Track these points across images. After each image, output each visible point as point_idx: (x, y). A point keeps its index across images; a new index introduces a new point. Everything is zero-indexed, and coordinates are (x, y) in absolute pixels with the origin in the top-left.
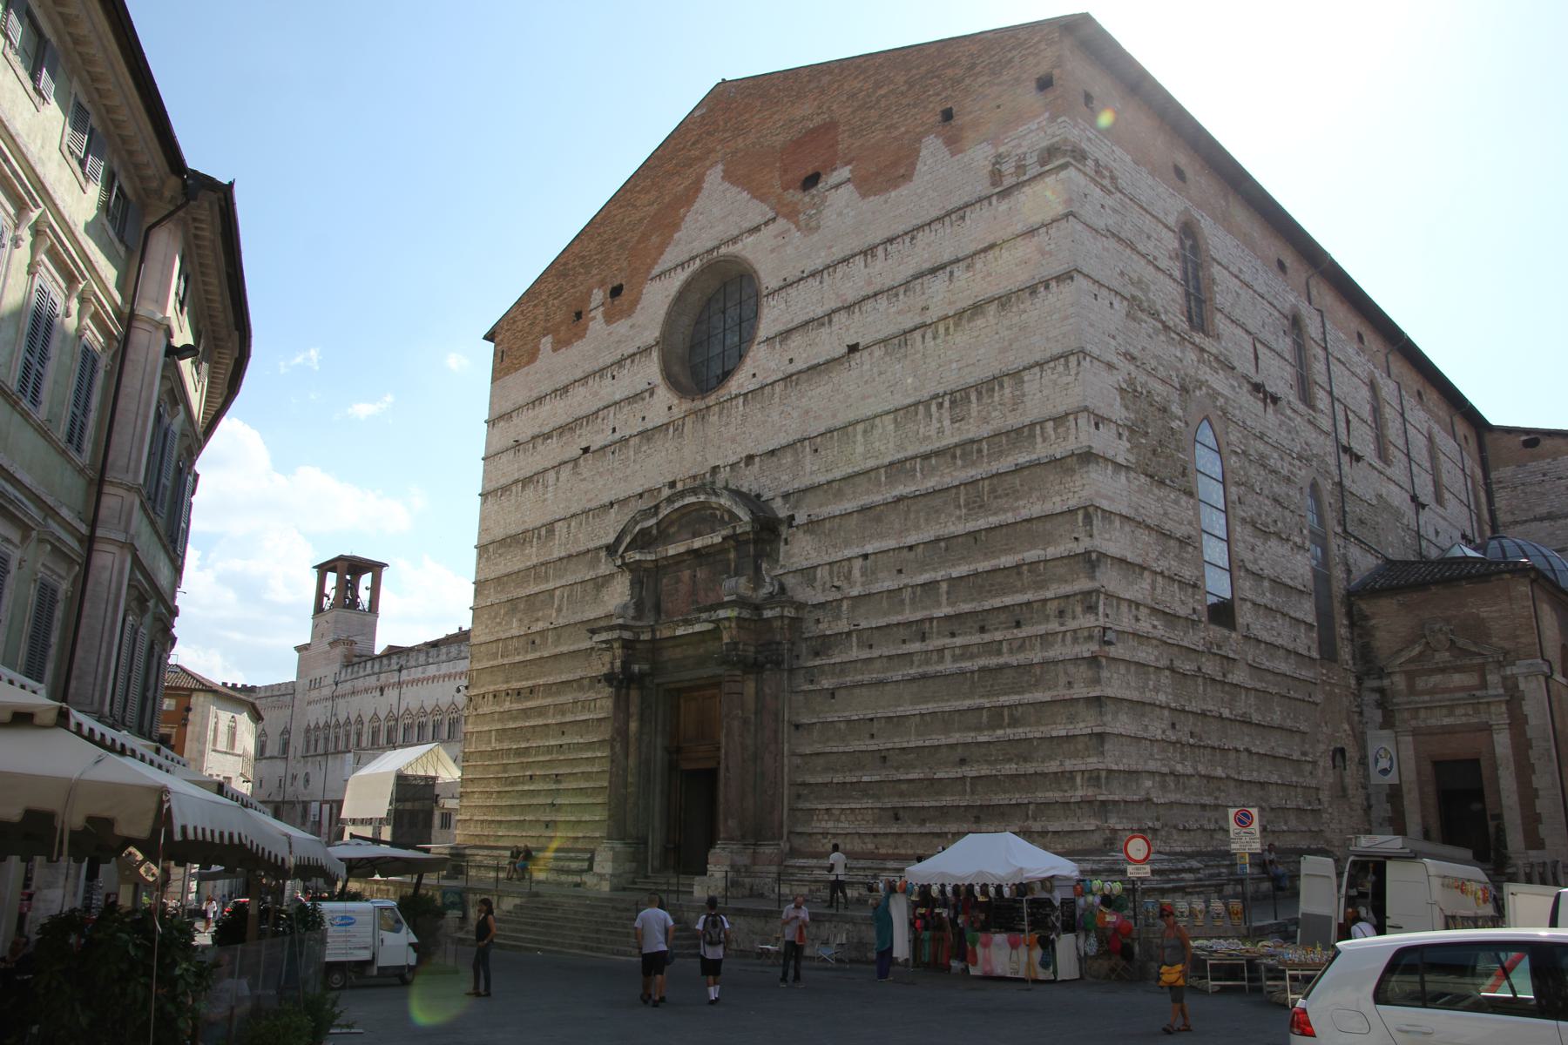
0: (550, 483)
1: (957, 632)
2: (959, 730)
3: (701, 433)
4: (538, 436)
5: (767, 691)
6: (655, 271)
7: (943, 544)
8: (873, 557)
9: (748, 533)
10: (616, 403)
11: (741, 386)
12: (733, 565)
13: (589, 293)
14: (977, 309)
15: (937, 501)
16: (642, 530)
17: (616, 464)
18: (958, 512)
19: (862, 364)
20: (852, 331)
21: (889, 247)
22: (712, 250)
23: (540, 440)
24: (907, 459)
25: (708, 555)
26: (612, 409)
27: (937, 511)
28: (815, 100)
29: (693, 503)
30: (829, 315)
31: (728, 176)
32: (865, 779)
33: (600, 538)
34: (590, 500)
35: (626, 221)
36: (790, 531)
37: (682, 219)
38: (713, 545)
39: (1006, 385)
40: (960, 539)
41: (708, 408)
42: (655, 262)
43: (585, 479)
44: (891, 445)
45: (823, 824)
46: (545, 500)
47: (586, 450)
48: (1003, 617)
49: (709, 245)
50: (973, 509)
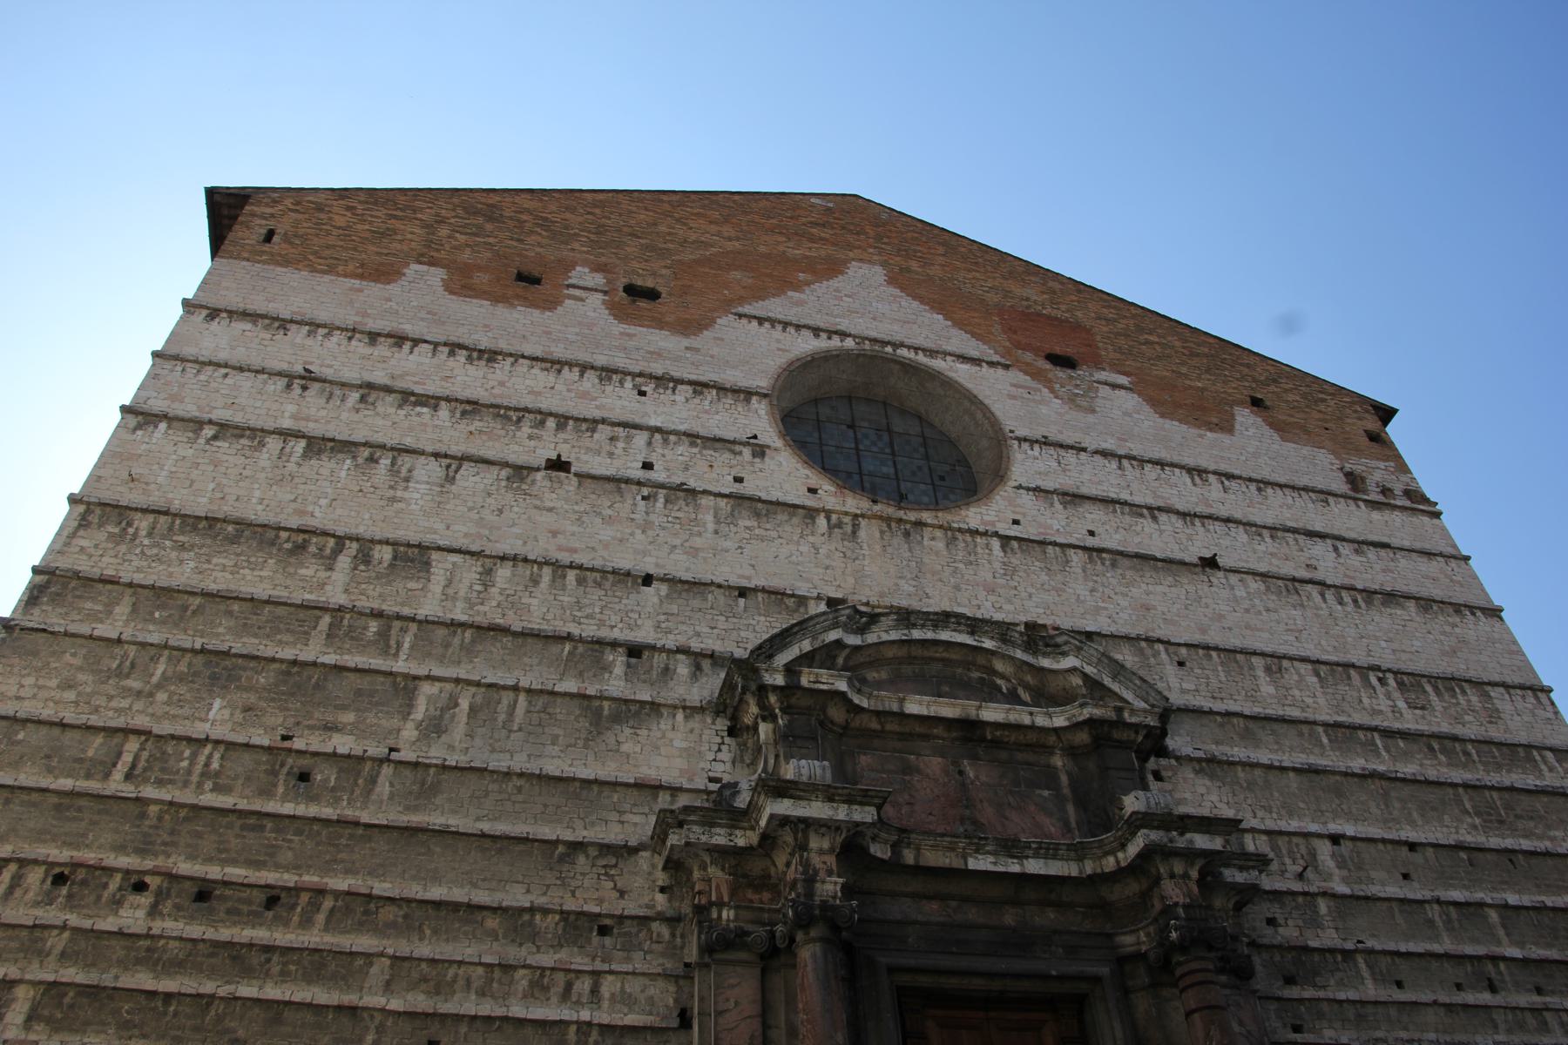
0: (420, 473)
3: (908, 554)
4: (388, 390)
5: (1236, 1028)
6: (747, 309)
7: (1463, 855)
8: (1349, 844)
9: (1136, 727)
10: (658, 430)
11: (993, 524)
12: (1064, 779)
13: (569, 266)
14: (1391, 598)
16: (838, 643)
17: (652, 517)
18: (1469, 820)
19: (1232, 588)
20: (1198, 544)
21: (1226, 483)
22: (885, 343)
23: (390, 399)
24: (1361, 727)
25: (996, 744)
26: (640, 438)
27: (1433, 809)
28: (1043, 293)
29: (949, 645)
30: (1150, 508)
31: (891, 281)
33: (601, 624)
34: (574, 551)
35: (663, 228)
36: (1163, 762)
37: (808, 284)
38: (1032, 727)
40: (1489, 856)
41: (919, 524)
42: (742, 300)
43: (550, 510)
44: (1321, 701)
46: (393, 500)
47: (558, 465)
49: (873, 334)
50: (1491, 821)
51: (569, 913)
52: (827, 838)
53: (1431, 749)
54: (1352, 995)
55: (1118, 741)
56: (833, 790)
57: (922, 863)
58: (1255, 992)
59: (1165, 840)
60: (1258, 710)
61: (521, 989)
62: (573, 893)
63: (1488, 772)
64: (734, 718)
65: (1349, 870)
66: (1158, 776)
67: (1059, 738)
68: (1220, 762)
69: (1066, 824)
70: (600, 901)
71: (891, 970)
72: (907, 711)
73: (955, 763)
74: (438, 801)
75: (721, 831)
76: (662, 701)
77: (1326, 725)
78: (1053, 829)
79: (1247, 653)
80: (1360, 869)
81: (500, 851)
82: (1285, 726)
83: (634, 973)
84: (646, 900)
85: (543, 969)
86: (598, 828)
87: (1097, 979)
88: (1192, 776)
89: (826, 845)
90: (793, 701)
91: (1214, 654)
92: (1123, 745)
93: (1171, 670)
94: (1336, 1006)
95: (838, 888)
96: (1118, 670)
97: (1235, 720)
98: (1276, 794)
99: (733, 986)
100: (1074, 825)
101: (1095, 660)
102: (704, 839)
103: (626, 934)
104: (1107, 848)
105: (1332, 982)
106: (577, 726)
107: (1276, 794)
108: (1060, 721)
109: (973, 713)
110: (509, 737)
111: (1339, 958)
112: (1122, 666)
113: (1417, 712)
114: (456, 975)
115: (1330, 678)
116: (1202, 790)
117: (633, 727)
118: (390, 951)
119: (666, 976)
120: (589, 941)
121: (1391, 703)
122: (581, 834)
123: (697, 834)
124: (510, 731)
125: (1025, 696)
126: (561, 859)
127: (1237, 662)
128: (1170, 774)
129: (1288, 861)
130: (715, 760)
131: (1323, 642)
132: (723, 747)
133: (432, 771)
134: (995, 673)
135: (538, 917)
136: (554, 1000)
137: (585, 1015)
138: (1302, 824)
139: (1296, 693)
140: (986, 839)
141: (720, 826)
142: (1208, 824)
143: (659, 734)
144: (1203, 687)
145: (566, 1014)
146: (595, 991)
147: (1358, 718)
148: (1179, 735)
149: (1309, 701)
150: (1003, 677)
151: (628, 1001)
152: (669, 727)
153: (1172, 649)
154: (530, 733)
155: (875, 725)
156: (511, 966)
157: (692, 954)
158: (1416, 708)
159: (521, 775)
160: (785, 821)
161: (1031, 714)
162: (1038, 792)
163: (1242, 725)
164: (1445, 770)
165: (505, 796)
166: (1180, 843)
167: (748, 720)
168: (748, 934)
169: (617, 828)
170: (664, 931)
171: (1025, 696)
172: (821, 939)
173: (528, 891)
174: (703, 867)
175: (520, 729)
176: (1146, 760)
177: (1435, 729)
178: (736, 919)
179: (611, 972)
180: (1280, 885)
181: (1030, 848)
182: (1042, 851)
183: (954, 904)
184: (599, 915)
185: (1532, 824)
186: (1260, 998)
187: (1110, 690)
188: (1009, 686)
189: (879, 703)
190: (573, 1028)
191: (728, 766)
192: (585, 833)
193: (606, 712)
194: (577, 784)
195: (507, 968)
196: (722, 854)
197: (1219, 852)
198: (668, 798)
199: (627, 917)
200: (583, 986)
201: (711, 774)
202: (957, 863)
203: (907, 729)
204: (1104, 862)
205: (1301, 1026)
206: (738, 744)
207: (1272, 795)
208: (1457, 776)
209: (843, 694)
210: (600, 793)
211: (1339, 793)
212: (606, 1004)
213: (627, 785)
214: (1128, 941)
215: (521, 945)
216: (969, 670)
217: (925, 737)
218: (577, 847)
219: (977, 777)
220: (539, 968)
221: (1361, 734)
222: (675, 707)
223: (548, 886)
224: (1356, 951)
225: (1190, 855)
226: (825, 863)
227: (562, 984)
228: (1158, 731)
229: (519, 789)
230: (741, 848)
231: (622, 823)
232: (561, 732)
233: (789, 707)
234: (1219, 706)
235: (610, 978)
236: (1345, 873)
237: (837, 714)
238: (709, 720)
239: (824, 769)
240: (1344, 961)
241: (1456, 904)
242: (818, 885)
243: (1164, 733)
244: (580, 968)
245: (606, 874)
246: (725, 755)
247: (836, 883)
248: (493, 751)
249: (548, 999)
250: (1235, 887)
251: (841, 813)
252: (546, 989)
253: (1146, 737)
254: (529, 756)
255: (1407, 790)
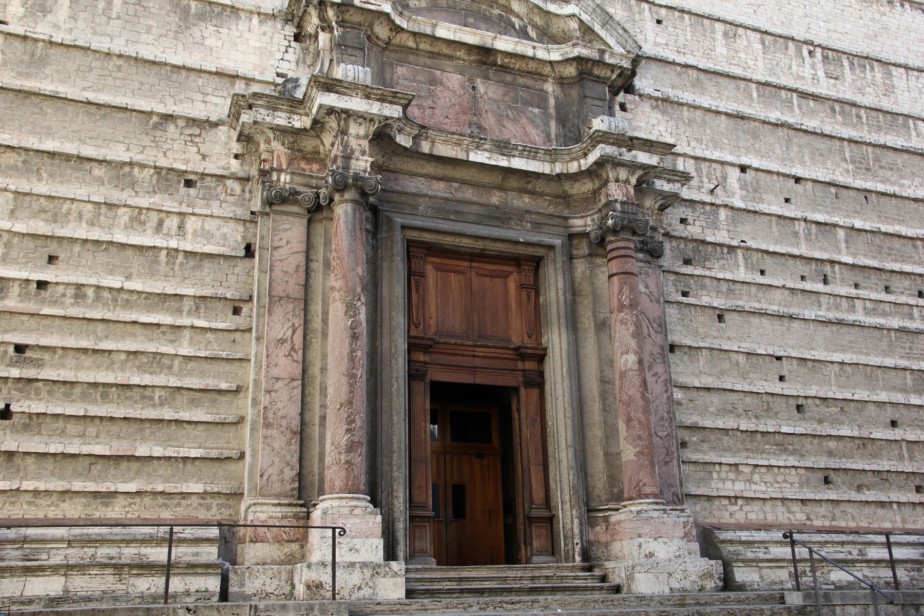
1: (860, 283)
2: (884, 388)
5: (642, 288)
7: (833, 190)
8: (753, 173)
9: (612, 67)
12: (552, 102)
15: (823, 144)
18: (845, 166)
25: (504, 69)
27: (822, 155)
32: (784, 429)
36: (630, 97)
38: (533, 59)
39: (876, 69)
40: (851, 193)
44: (760, 64)
45: (729, 484)
48: (907, 283)
50: (861, 168)
51: (161, 168)
52: (363, 127)
53: (833, 110)
54: (728, 276)
55: (598, 77)
56: (369, 90)
57: (435, 153)
58: (661, 267)
59: (616, 154)
60: (709, 65)
61: (123, 222)
62: (165, 155)
63: (870, 132)
64: (299, 26)
65: (748, 191)
66: (623, 107)
67: (553, 69)
68: (671, 102)
69: (548, 135)
70: (187, 161)
71: (404, 227)
72: (437, 35)
73: (471, 80)
74: (48, 71)
75: (283, 115)
76: (241, 6)
77: (759, 83)
78: (537, 138)
79: (712, 19)
80: (756, 191)
81: (104, 116)
82: (728, 80)
83: (212, 216)
84: (223, 163)
85: (141, 209)
86: (185, 105)
87: (551, 247)
88: (649, 110)
89: (362, 132)
90: (347, 16)
91: (686, 17)
92: (599, 80)
93: (650, 25)
94: (715, 282)
95: (369, 165)
96: (608, 20)
97: (690, 71)
98: (708, 131)
99: (286, 230)
100: (553, 136)
101: (591, 10)
102: (268, 119)
103: (206, 187)
104: (574, 155)
105: (717, 266)
106: (168, 19)
107: (708, 131)
108: (555, 56)
109: (488, 43)
110: (108, 23)
111: (725, 250)
112: (611, 17)
113: (832, 81)
114: (70, 209)
115: (772, 47)
116: (654, 122)
117: (216, 26)
118: (13, 188)
119: (237, 220)
120: (177, 190)
121: (813, 72)
122: (170, 109)
123: (262, 114)
124: (110, 18)
125: (532, 33)
126: (156, 127)
127: (703, 25)
128: (633, 107)
129: (705, 180)
130: (282, 59)
131: (775, 17)
132: (289, 50)
133: (40, 45)
134: (511, 12)
135: (136, 170)
136: (149, 231)
137: (173, 244)
138: (722, 155)
139: (742, 55)
140: (485, 139)
141: (281, 110)
142: (649, 145)
143: (237, 34)
144: (672, 42)
145: (159, 242)
146: (181, 227)
147: (784, 81)
148: (646, 78)
149: (751, 63)
150: (517, 16)
151: (207, 235)
152: (247, 29)
153: (654, 9)
154: (127, 22)
155: (411, 44)
156: (114, 205)
157: (257, 205)
158: (831, 78)
159: (120, 56)
160: (331, 111)
161: (534, 48)
162: (531, 109)
163: (695, 76)
164: (839, 127)
165: (108, 73)
166: (627, 156)
167: (310, 29)
168: (297, 193)
169: (202, 106)
170: (237, 187)
171: (532, 33)
172: (354, 201)
173: (128, 150)
174: (268, 141)
175: (118, 18)
176: (616, 94)
177: (841, 96)
178: (291, 182)
179: (194, 214)
180: (696, 196)
181: (517, 149)
182: (526, 153)
183: (456, 185)
184: (186, 172)
185: (890, 173)
186: (663, 271)
187: (598, 36)
188: (521, 23)
189: (416, 26)
190: (164, 252)
191: (293, 65)
192: (175, 108)
193: (193, 11)
194: (169, 68)
195: (110, 206)
196: (282, 132)
197: (654, 167)
198: (243, 86)
199: (207, 175)
200: (172, 223)
201: (279, 71)
202: (461, 155)
203: (436, 50)
204: (570, 165)
205: (688, 292)
206: (302, 48)
207: (705, 131)
208: (846, 133)
209: (388, 15)
210: (188, 77)
211: (755, 136)
212: (189, 237)
213: (210, 73)
214: (578, 224)
215: (123, 190)
216: (491, 7)
217: (450, 57)
218: (168, 118)
219: (486, 93)
220: (137, 207)
221: (783, 93)
222: (251, 13)
223: (144, 147)
224: (738, 247)
225: (633, 166)
226: (360, 145)
227: (156, 221)
228: (629, 72)
229: (119, 68)
230: (298, 129)
231: (206, 102)
232: (154, 23)
233: (343, 21)
234: (680, 59)
235: (193, 218)
236: (744, 193)
237: (382, 31)
238: (279, 26)
239: (366, 74)
240: (728, 253)
241: (818, 223)
242: (353, 162)
243: (634, 74)
244: (170, 209)
245: (192, 141)
246: (291, 56)
247: (367, 161)
248: (95, 33)
249: (144, 231)
250: (661, 194)
251: (375, 108)
252: (143, 223)
253: (619, 76)
254: (127, 41)
255: (807, 138)
